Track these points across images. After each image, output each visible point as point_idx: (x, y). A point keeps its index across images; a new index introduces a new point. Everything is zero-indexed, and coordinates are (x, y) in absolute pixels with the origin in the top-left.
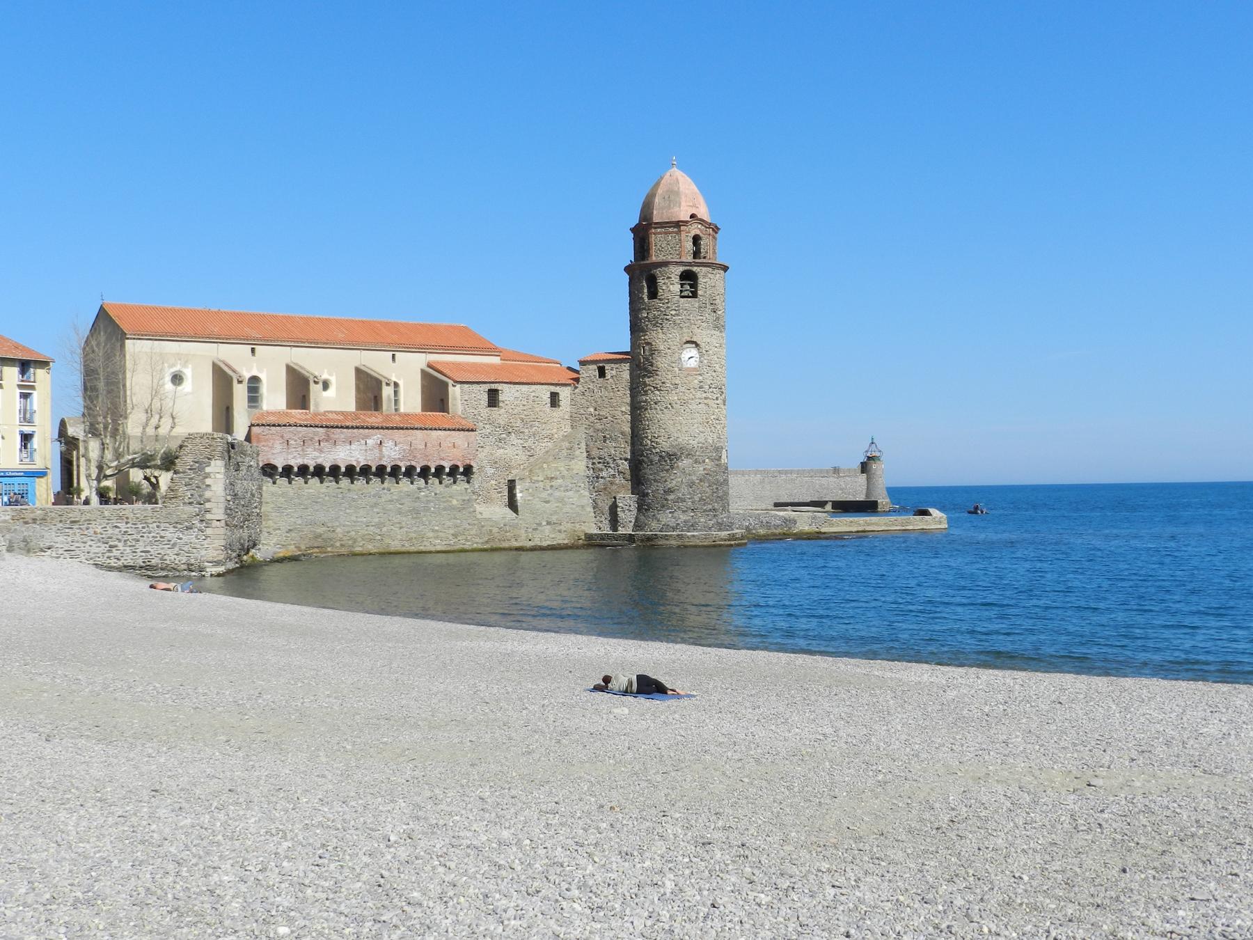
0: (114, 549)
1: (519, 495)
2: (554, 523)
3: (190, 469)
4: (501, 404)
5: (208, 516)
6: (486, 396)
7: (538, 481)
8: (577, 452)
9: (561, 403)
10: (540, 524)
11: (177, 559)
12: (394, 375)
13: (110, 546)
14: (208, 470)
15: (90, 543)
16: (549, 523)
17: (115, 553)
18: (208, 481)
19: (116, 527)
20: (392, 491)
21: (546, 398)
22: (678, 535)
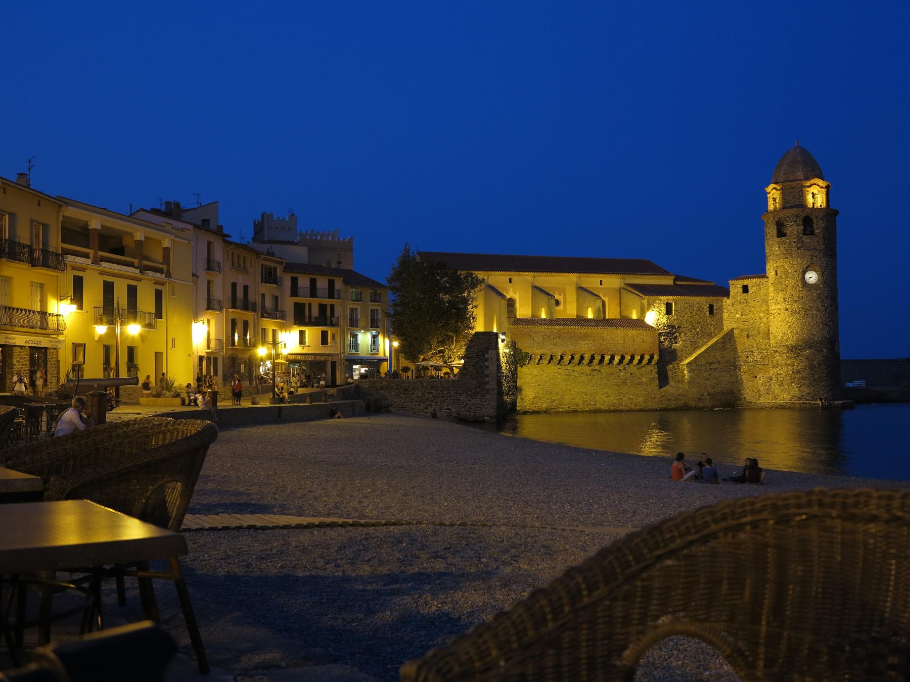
0: (429, 407)
3: (475, 356)
5: (487, 387)
7: (701, 365)
8: (728, 346)
10: (703, 395)
11: (468, 414)
12: (601, 294)
13: (427, 405)
14: (486, 356)
15: (415, 403)
18: (487, 364)
19: (431, 393)
20: (602, 371)
22: (804, 403)
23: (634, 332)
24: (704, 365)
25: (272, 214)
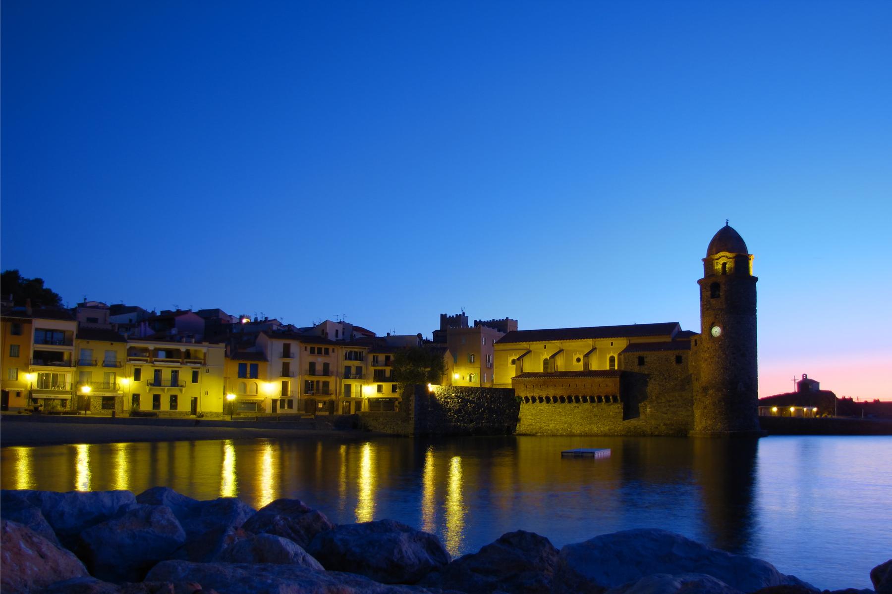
1: (649, 410)
2: (668, 425)
4: (646, 363)
6: (637, 361)
7: (661, 403)
8: (687, 387)
9: (683, 361)
10: (659, 425)
14: (411, 398)
16: (665, 424)
17: (386, 429)
18: (410, 403)
21: (673, 359)
23: (600, 379)
24: (664, 402)
25: (446, 315)
